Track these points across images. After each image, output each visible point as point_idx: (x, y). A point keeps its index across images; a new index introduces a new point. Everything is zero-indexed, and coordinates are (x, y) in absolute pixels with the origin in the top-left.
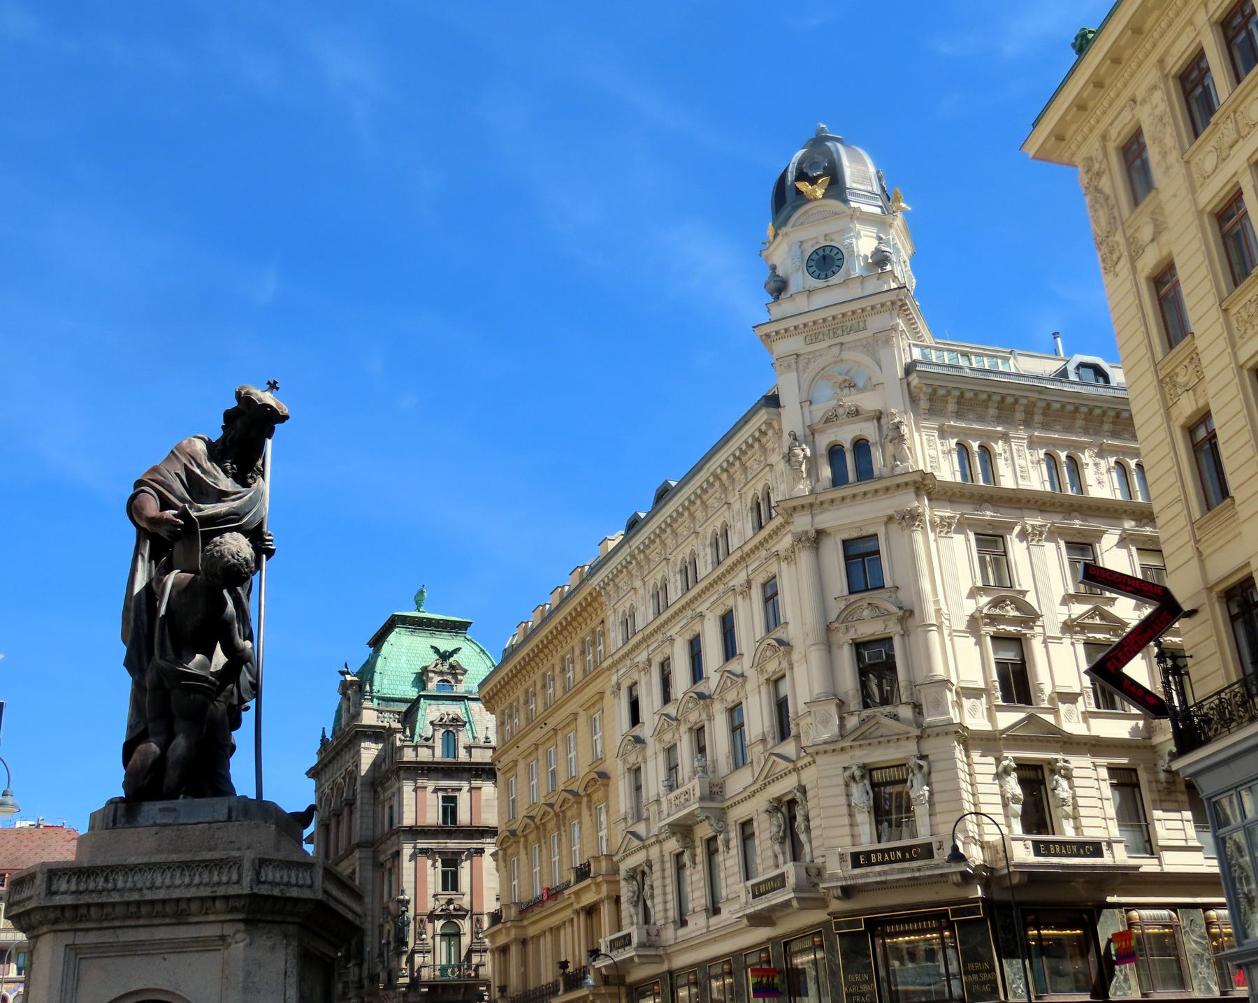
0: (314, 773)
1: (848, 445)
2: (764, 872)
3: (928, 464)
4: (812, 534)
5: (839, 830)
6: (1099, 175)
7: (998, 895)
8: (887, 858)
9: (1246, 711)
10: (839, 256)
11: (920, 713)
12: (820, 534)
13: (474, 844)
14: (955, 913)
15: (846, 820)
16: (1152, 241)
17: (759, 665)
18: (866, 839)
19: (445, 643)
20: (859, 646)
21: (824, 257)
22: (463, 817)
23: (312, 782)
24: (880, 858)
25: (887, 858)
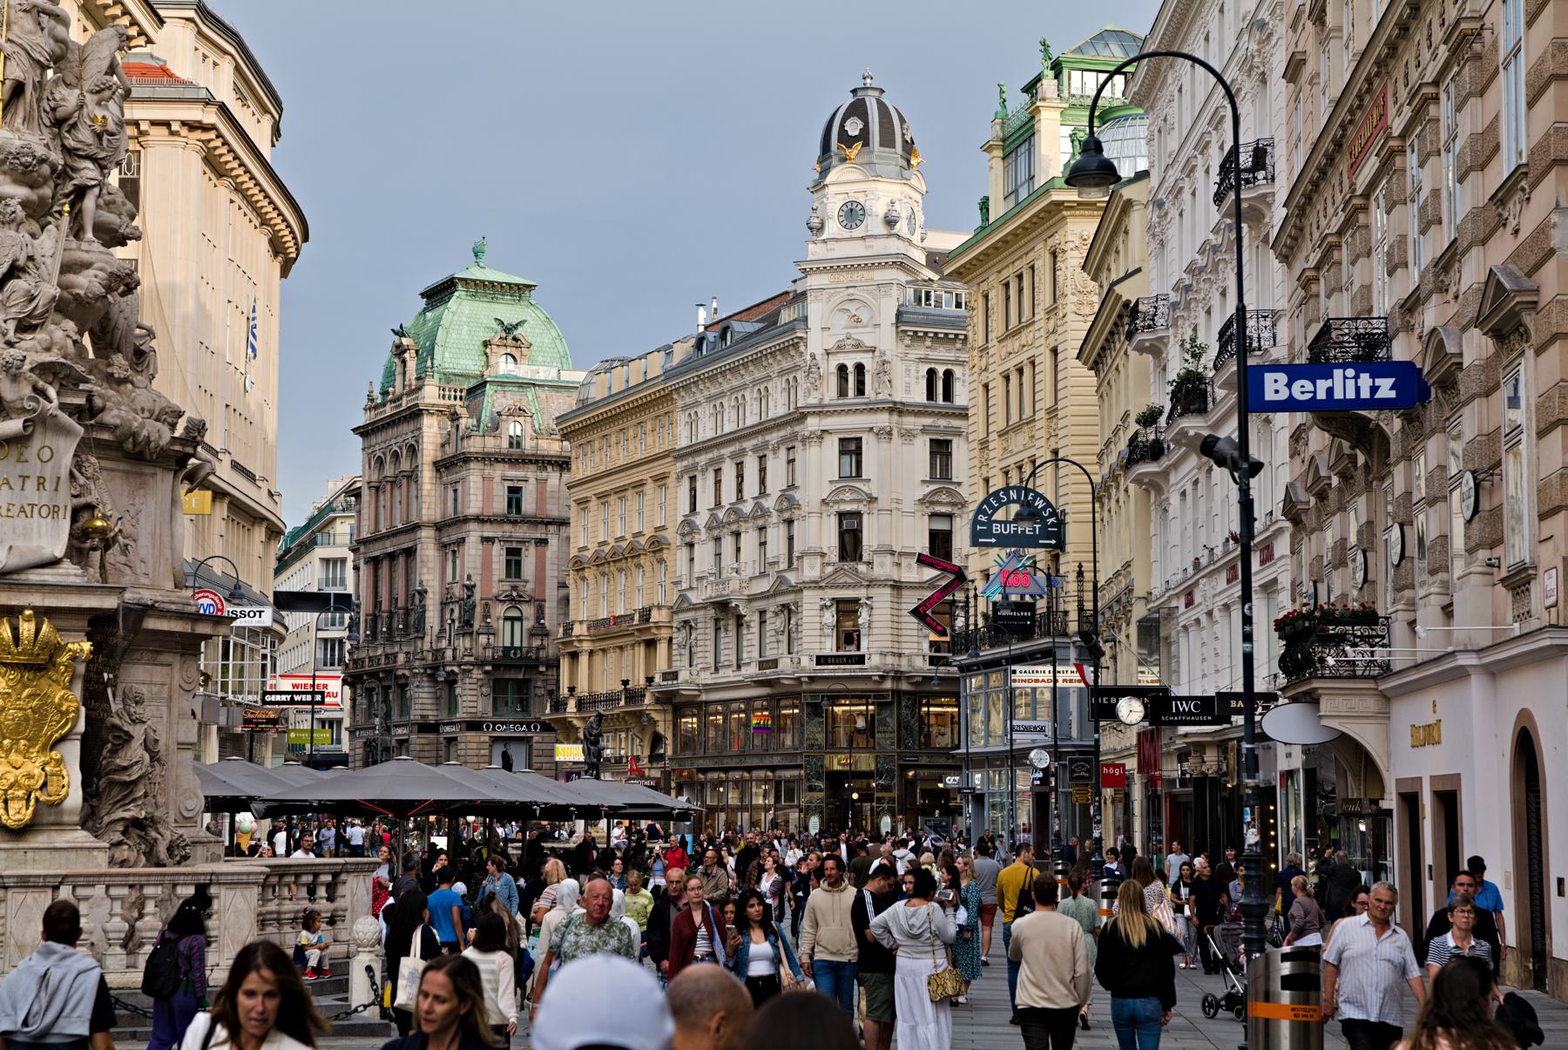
0: (364, 432)
5: (816, 634)
7: (904, 686)
13: (539, 533)
18: (829, 648)
19: (509, 311)
20: (842, 516)
22: (528, 506)
23: (359, 439)
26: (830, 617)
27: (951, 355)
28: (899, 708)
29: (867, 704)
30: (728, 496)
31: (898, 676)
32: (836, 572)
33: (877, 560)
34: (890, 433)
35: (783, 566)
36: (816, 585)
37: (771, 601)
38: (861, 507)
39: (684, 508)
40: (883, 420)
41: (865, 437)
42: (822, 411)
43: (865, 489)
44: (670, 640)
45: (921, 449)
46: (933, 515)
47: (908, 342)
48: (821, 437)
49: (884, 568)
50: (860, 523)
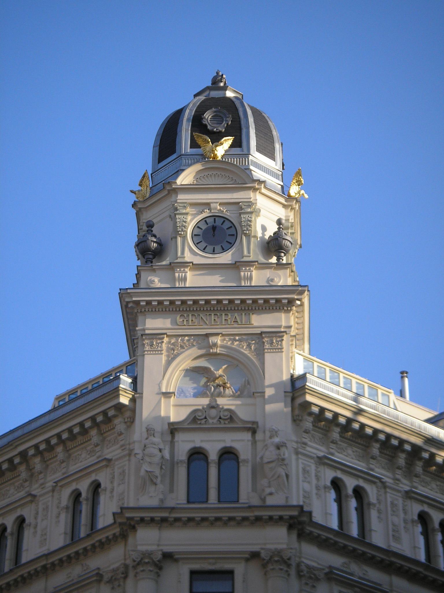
1: (213, 456)
3: (301, 499)
4: (159, 556)
10: (232, 231)
12: (168, 556)
21: (214, 228)
27: (361, 465)
40: (277, 538)
41: (239, 569)
42: (164, 519)
47: (308, 423)
48: (159, 567)
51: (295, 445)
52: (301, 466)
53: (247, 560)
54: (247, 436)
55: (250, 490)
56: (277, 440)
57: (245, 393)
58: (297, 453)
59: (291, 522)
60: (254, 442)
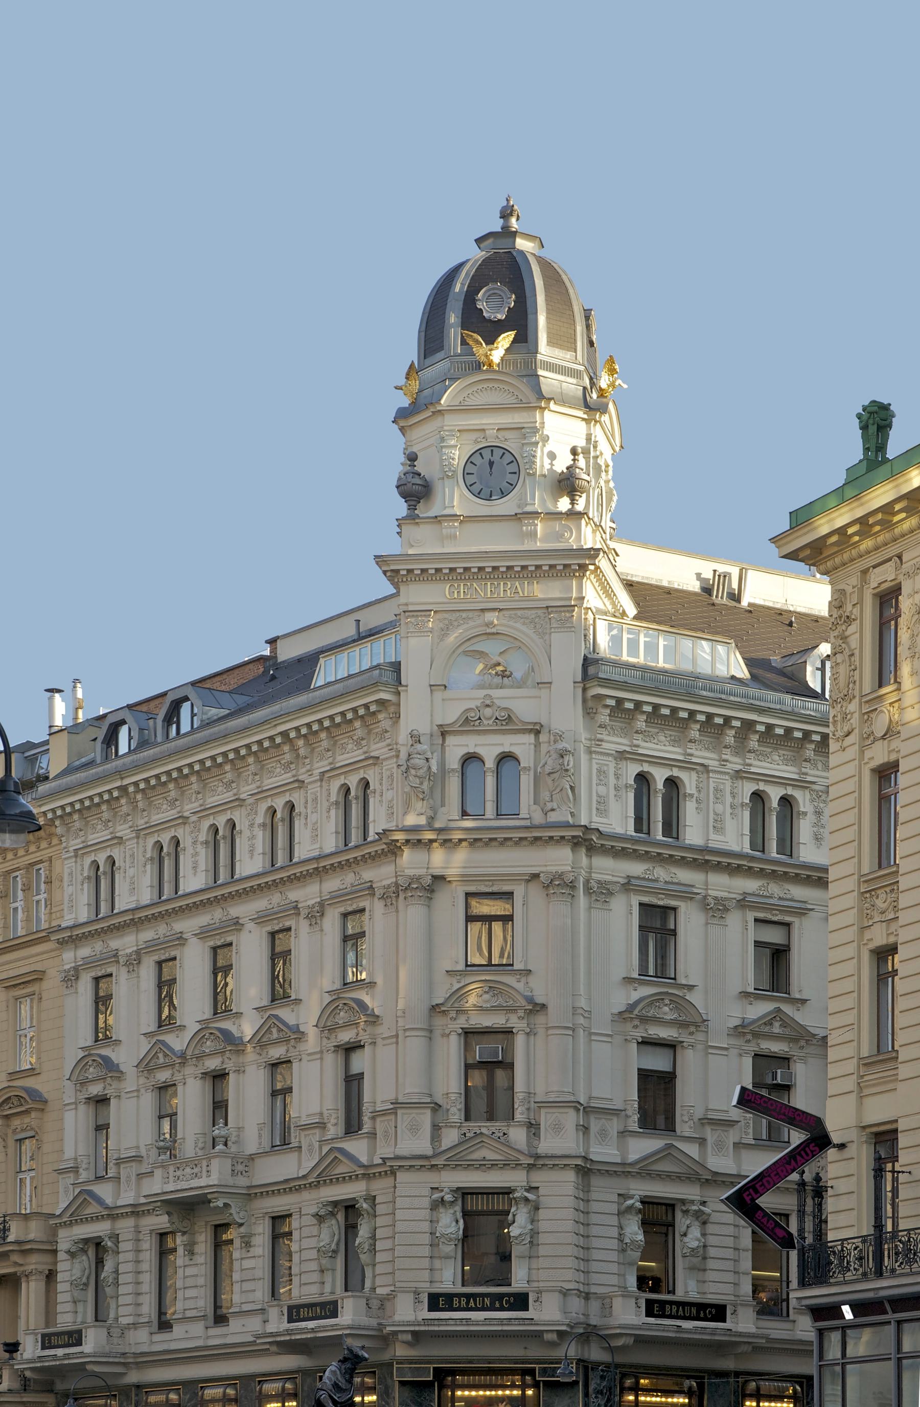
2: (304, 1288)
5: (414, 1254)
6: (849, 620)
8: (472, 1304)
9: (861, 1266)
11: (537, 1135)
14: (544, 1371)
15: (426, 1251)
16: (883, 738)
17: (327, 1028)
18: (449, 1279)
24: (463, 1303)
25: (472, 1304)
26: (450, 1223)
28: (586, 1395)
29: (523, 1387)
30: (193, 1003)
31: (589, 1334)
32: (464, 1139)
33: (546, 1119)
34: (572, 886)
35: (335, 1129)
36: (423, 1163)
37: (306, 1195)
38: (515, 1022)
39: (85, 1037)
40: (560, 859)
41: (519, 891)
43: (520, 986)
44: (51, 1276)
45: (622, 921)
46: (645, 1043)
49: (560, 1139)
50: (509, 1049)
51: (588, 743)
52: (595, 767)
53: (528, 881)
54: (531, 738)
55: (532, 802)
56: (561, 745)
57: (529, 682)
58: (590, 752)
59: (575, 841)
60: (537, 745)
